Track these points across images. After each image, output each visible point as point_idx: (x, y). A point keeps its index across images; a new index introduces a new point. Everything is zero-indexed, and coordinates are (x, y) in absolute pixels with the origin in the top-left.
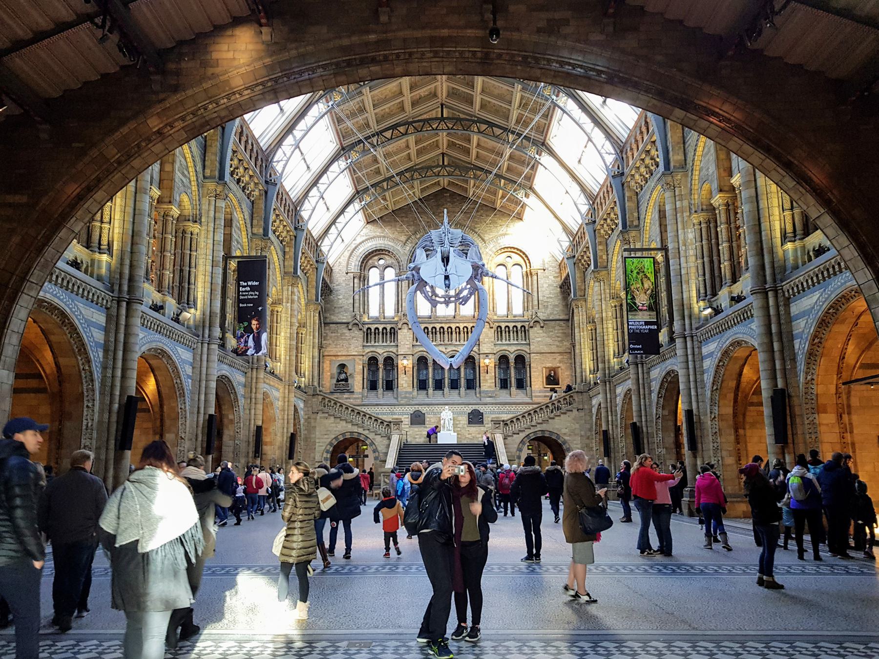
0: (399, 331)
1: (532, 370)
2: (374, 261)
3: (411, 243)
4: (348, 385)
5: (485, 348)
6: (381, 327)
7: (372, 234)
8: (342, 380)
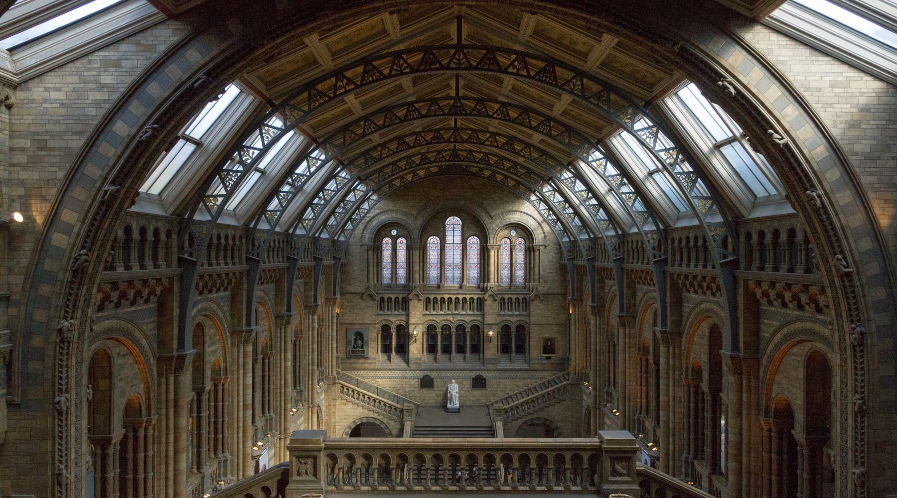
1: (531, 340)
4: (363, 352)
5: (489, 319)
7: (386, 208)
8: (358, 347)
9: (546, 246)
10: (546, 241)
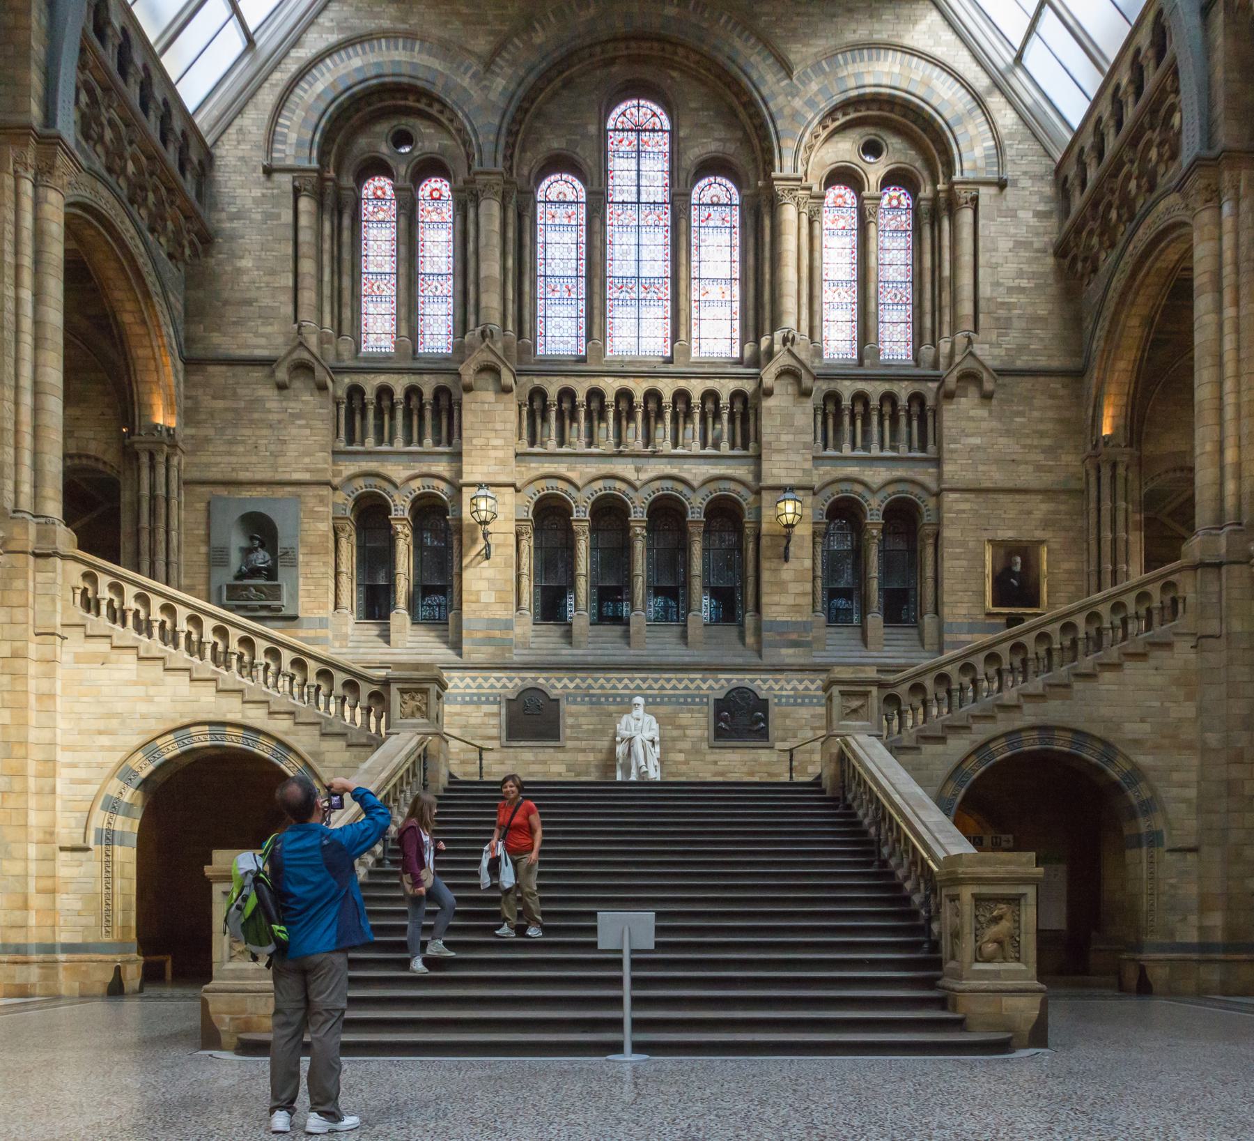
0: (466, 398)
1: (947, 551)
2: (377, 141)
3: (513, 63)
6: (399, 385)
7: (371, 25)
9: (1002, 185)
10: (1001, 164)
